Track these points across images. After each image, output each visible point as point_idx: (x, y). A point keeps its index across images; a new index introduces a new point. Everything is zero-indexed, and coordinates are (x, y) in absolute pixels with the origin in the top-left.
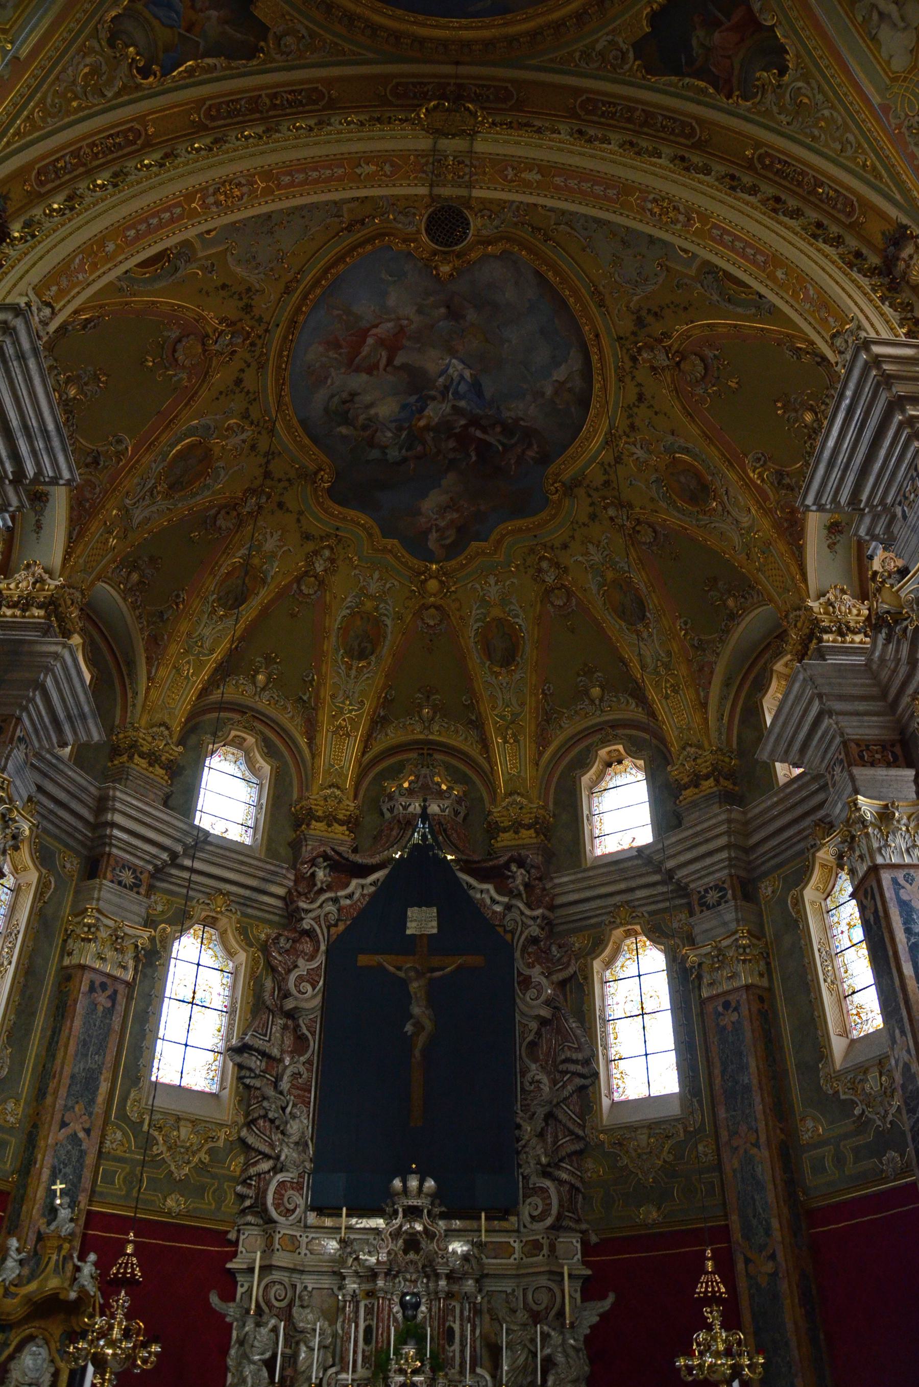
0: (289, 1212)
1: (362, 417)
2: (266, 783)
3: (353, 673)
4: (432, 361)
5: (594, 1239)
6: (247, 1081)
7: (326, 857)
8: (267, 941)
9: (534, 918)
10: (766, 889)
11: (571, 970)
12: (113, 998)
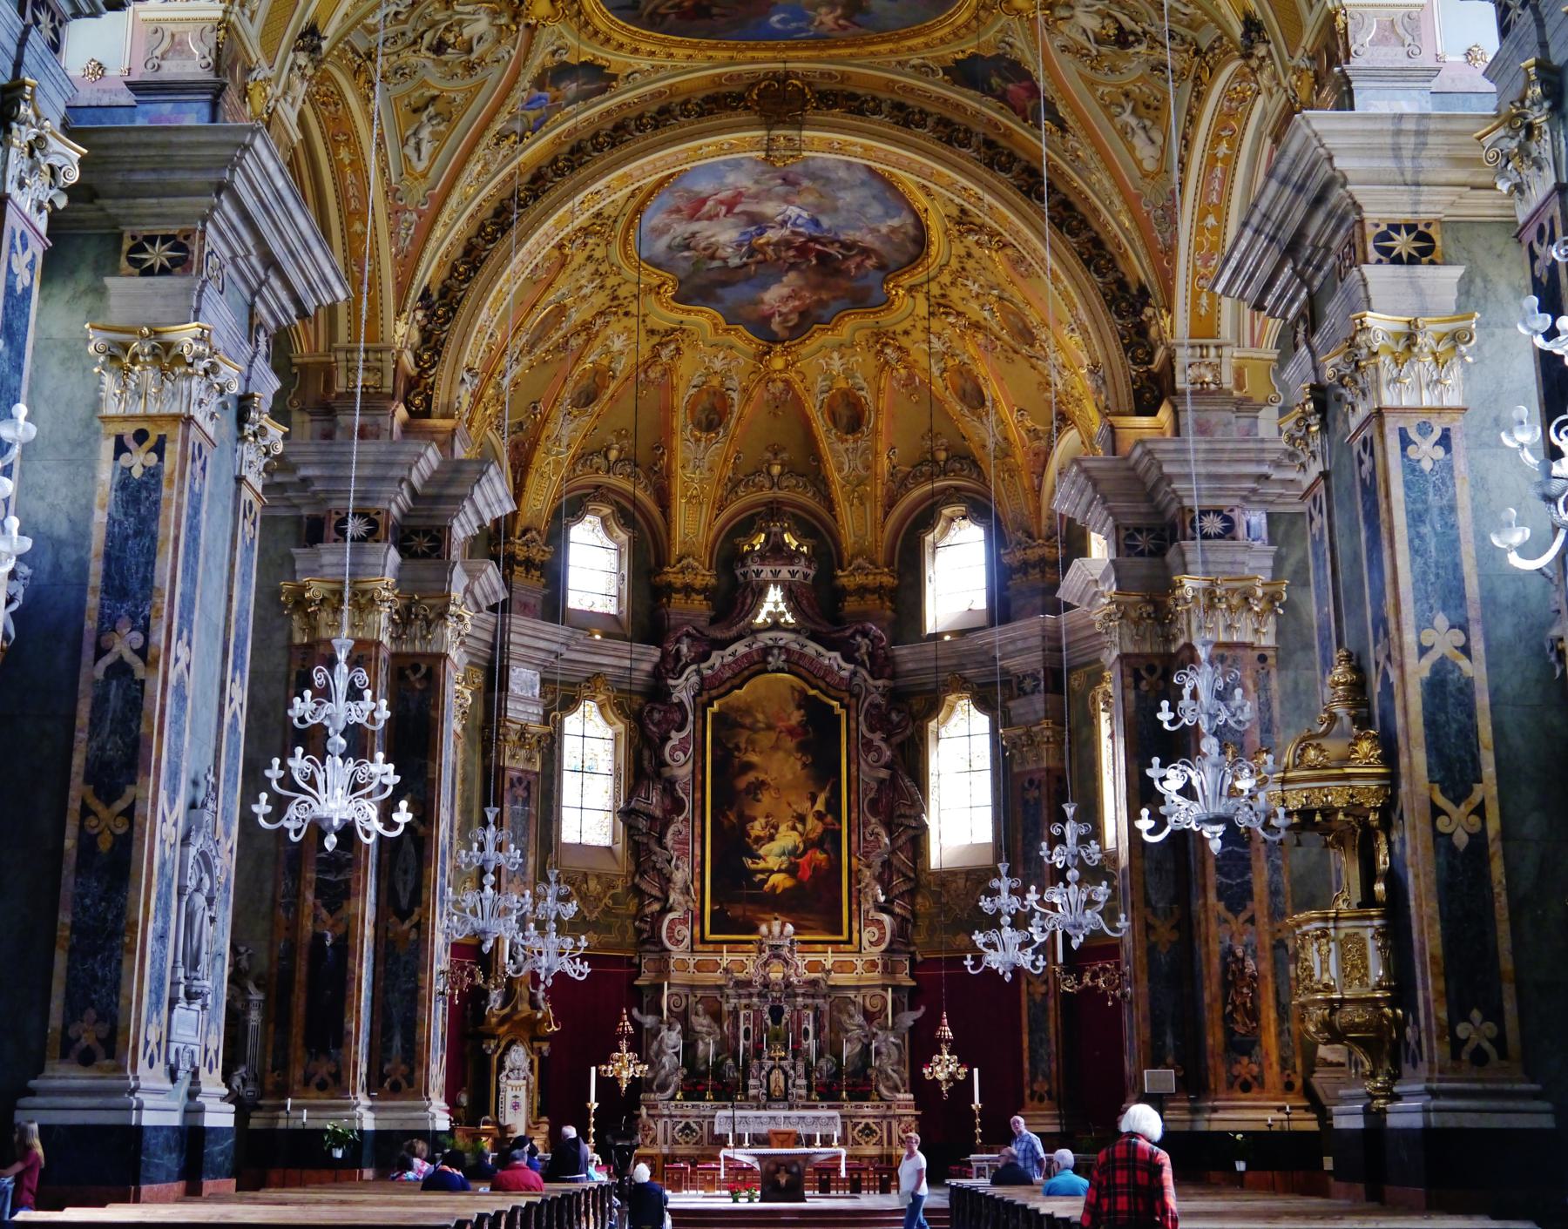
0: (678, 942)
1: (703, 245)
2: (625, 550)
3: (703, 444)
4: (770, 208)
5: (919, 958)
7: (688, 635)
8: (641, 710)
9: (877, 688)
10: (1076, 681)
11: (908, 732)
12: (527, 788)
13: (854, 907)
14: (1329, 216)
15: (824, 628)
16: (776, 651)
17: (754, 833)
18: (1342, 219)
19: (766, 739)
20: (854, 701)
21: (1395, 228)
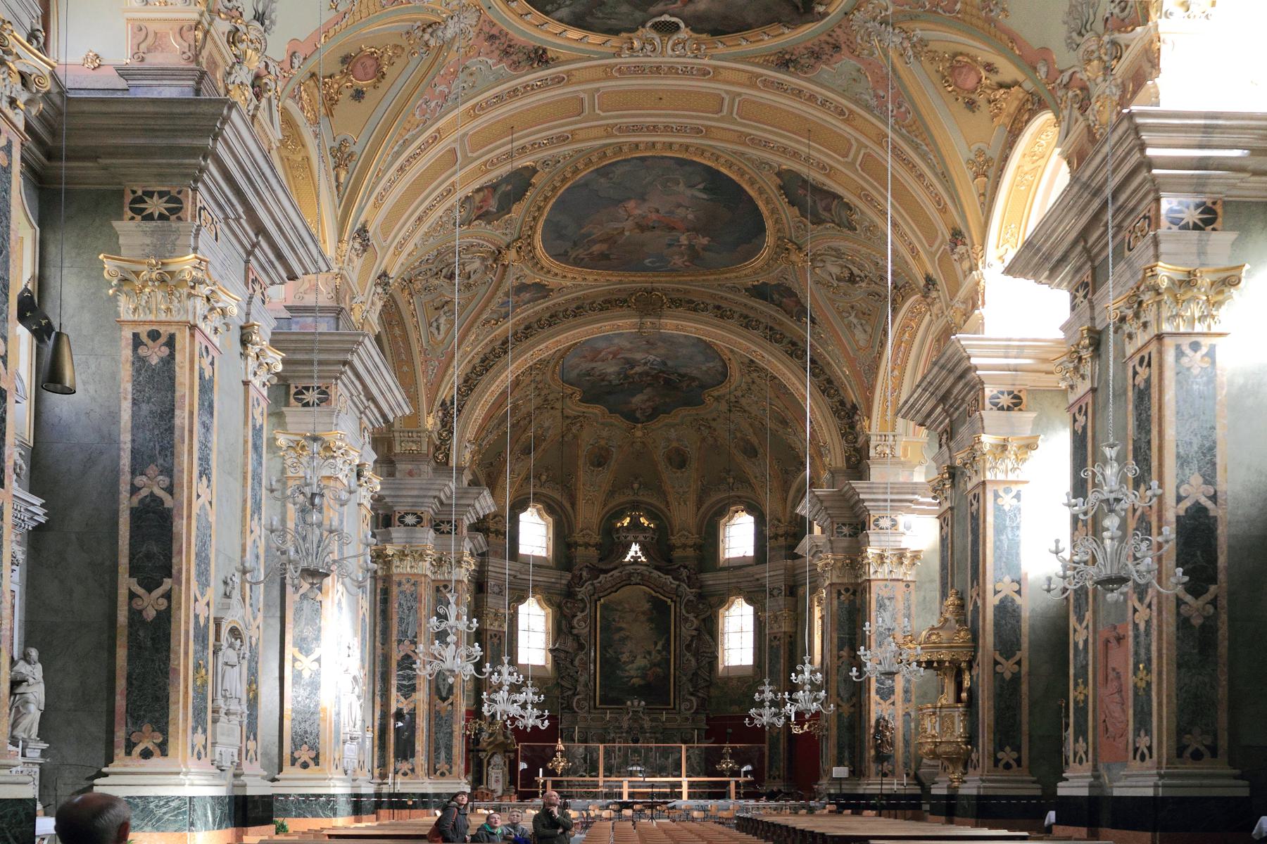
14: (966, 385)
15: (664, 563)
18: (973, 387)
21: (1002, 393)
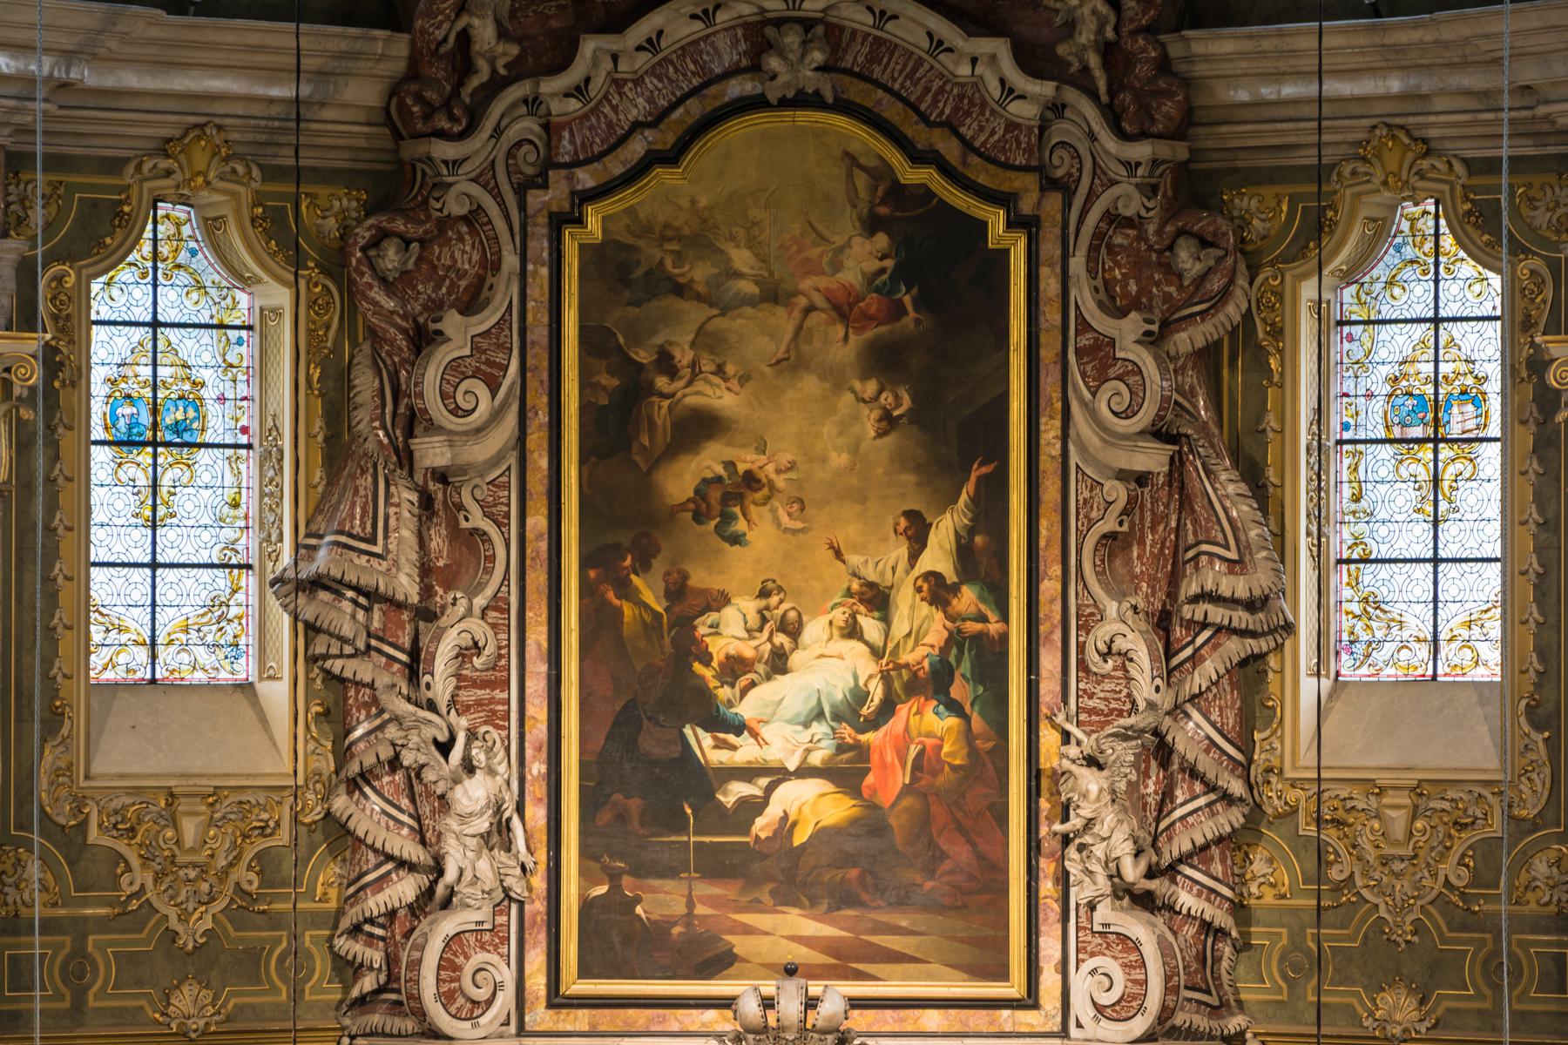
0: (478, 1007)
6: (336, 666)
9: (1131, 166)
11: (1232, 312)
13: (1047, 887)
16: (792, 39)
17: (719, 648)
19: (760, 335)
20: (1054, 201)
